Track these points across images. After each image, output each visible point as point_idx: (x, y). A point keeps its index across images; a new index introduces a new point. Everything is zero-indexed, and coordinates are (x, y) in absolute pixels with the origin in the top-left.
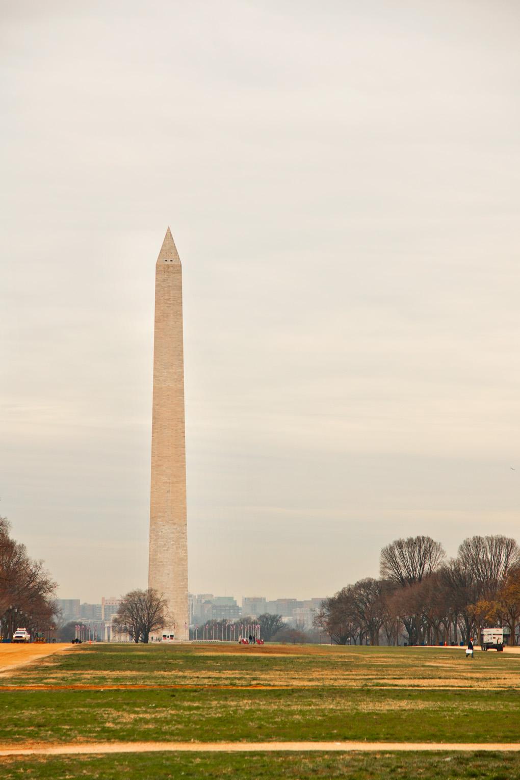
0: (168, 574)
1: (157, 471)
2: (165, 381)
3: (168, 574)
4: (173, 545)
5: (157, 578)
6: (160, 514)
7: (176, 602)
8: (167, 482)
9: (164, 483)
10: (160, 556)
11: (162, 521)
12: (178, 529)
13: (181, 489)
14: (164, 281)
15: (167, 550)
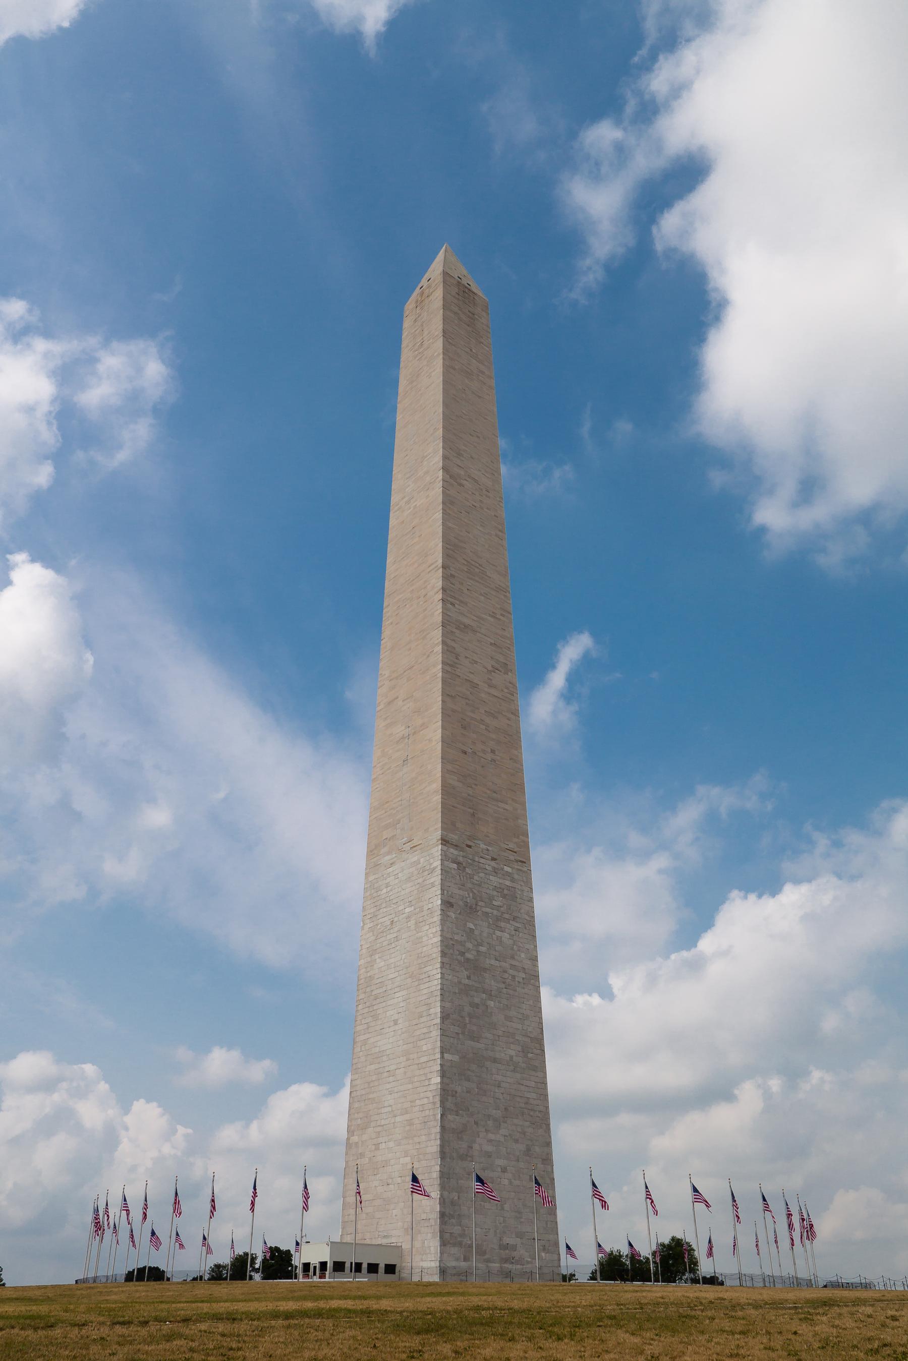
0: (396, 1022)
1: (386, 719)
2: (408, 502)
3: (396, 1022)
4: (409, 917)
5: (372, 1040)
6: (386, 834)
7: (410, 1123)
8: (403, 738)
9: (398, 742)
10: (382, 964)
11: (389, 853)
12: (422, 860)
13: (430, 740)
14: (415, 321)
15: (397, 939)
